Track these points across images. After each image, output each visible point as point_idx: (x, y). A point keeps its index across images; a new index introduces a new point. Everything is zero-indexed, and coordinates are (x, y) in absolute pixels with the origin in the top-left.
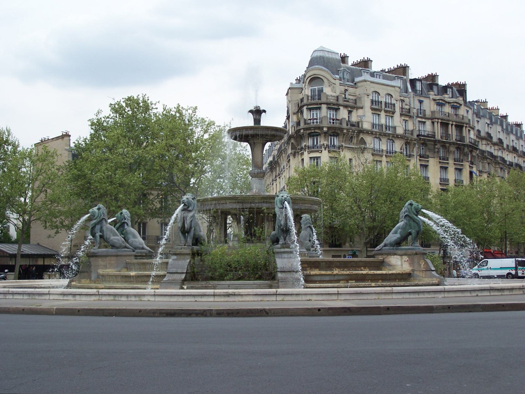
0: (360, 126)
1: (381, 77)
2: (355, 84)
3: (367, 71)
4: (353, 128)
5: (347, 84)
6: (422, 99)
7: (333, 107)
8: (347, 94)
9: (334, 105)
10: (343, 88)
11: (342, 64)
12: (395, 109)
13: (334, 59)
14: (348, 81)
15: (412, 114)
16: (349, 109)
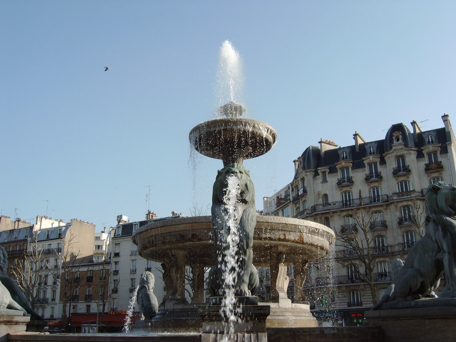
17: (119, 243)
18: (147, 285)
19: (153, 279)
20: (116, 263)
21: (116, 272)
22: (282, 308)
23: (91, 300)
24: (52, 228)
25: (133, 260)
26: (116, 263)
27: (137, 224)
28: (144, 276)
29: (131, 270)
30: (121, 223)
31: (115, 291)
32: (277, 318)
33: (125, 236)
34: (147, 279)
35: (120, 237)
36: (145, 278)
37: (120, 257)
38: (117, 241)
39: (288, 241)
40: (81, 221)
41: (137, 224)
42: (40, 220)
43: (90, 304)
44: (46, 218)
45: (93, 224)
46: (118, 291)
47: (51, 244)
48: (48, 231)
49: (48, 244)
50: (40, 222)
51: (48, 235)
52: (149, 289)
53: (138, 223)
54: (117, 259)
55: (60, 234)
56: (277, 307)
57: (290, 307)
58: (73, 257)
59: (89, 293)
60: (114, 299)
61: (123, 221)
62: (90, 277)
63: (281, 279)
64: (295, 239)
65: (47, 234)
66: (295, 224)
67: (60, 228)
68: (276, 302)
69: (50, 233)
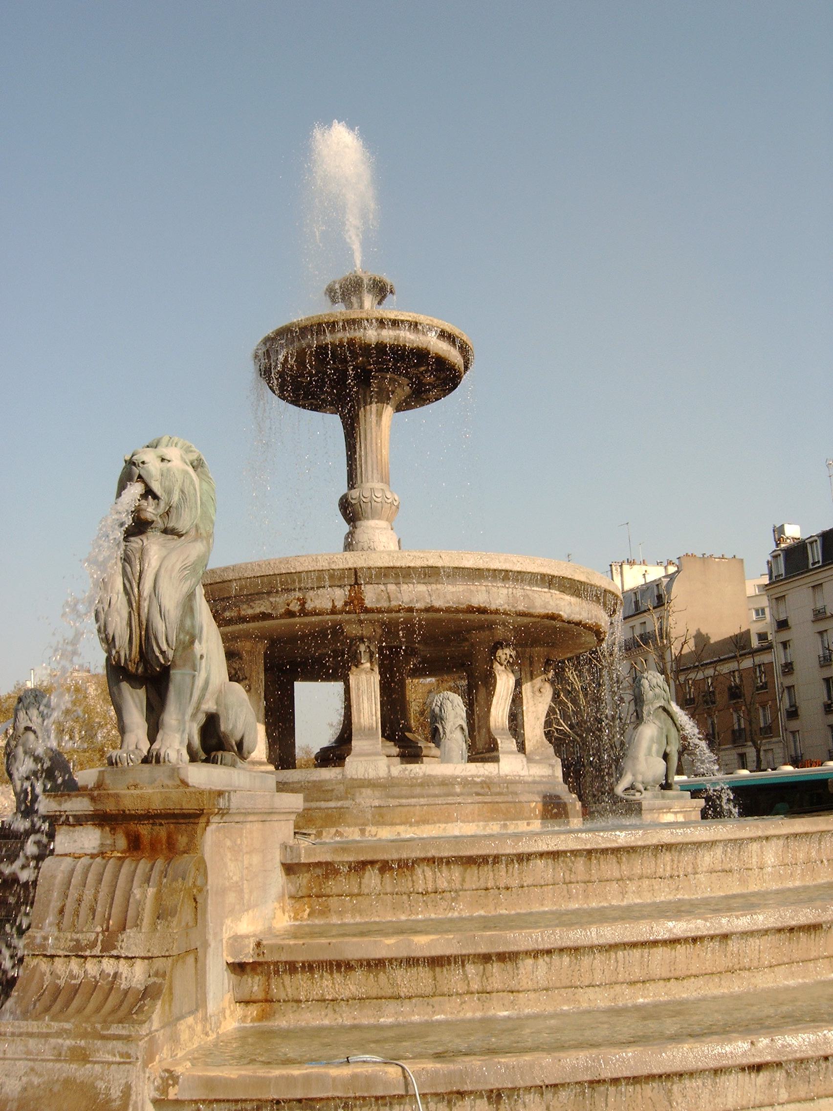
17: (784, 596)
18: (442, 723)
19: (458, 710)
20: (785, 645)
21: (788, 669)
22: (352, 779)
23: (746, 741)
24: (646, 584)
25: (821, 633)
26: (785, 645)
27: (816, 541)
28: (436, 705)
29: (819, 657)
30: (783, 545)
31: (793, 714)
32: (323, 804)
33: (799, 575)
34: (441, 711)
35: (782, 580)
36: (437, 709)
37: (790, 628)
38: (778, 591)
39: (314, 613)
40: (706, 556)
41: (816, 541)
42: (619, 570)
43: (744, 750)
44: (632, 563)
45: (737, 557)
46: (799, 713)
47: (645, 623)
48: (635, 593)
49: (641, 623)
50: (619, 575)
51: (636, 602)
52: (445, 733)
53: (816, 538)
54: (784, 636)
55: (660, 597)
56: (340, 777)
57: (382, 772)
58: (702, 639)
59: (765, 723)
60: (793, 733)
61: (788, 538)
62: (737, 687)
63: (366, 705)
64: (334, 607)
65: (633, 600)
66: (317, 568)
67: (657, 584)
68: (339, 766)
69: (639, 598)
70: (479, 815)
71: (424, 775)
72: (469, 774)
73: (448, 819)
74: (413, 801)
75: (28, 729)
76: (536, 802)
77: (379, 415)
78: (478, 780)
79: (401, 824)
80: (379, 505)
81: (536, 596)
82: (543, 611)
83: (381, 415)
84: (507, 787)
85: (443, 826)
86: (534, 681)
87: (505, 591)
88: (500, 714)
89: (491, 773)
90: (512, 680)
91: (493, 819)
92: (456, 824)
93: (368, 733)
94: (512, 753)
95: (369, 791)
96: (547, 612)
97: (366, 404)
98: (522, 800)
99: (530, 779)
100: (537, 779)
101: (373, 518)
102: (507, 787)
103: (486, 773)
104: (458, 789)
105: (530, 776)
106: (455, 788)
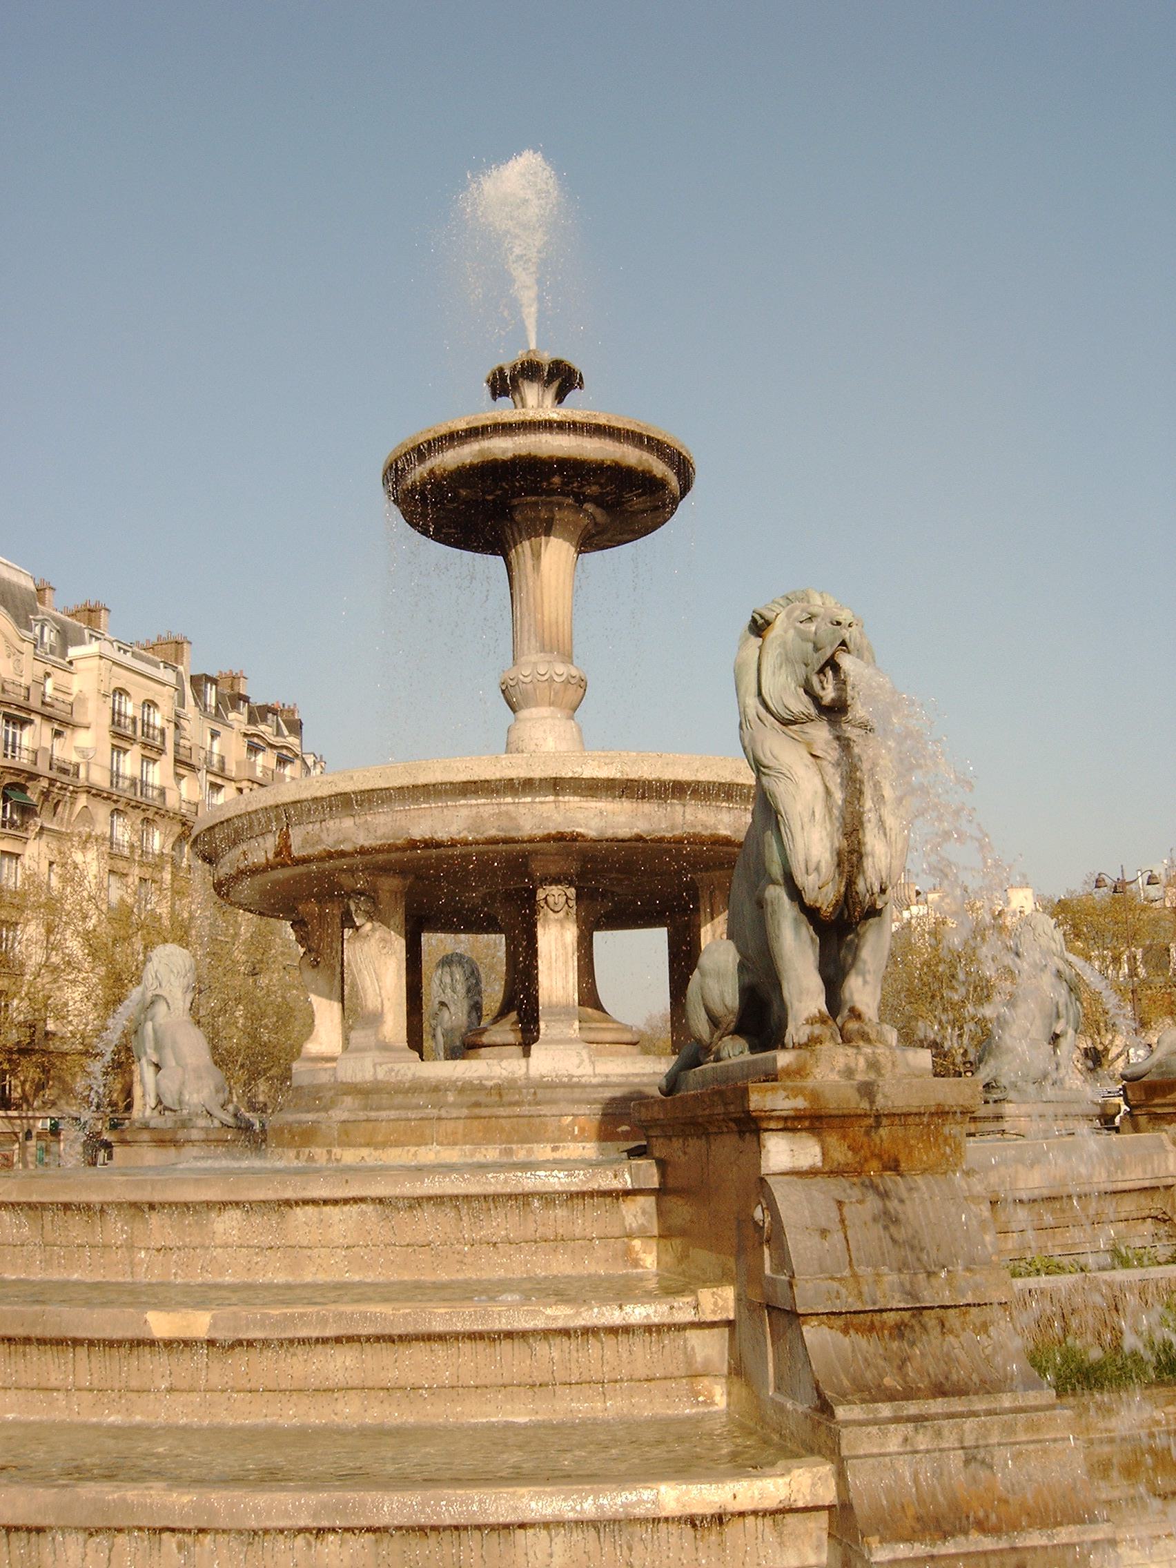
0: (82, 774)
1: (129, 654)
2: (71, 663)
3: (99, 636)
4: (65, 779)
5: (50, 660)
6: (217, 727)
7: (16, 713)
8: (49, 684)
9: (19, 707)
10: (40, 669)
11: (38, 604)
12: (163, 743)
13: (19, 587)
14: (52, 652)
15: (194, 761)
16: (56, 726)
56: (332, 1080)
70: (465, 1136)
71: (414, 1075)
72: (476, 1075)
73: (422, 1141)
74: (383, 1114)
75: (443, 1004)
76: (573, 1115)
77: (537, 556)
78: (490, 1083)
79: (368, 1145)
80: (530, 686)
81: (522, 810)
82: (540, 833)
83: (539, 555)
84: (535, 1093)
85: (413, 1149)
86: (716, 920)
87: (464, 812)
88: (560, 985)
89: (513, 1073)
90: (571, 933)
91: (489, 1141)
92: (431, 1147)
93: (562, 1012)
94: (570, 1041)
95: (348, 1100)
96: (546, 832)
97: (515, 545)
98: (548, 1114)
99: (595, 1081)
100: (614, 1079)
101: (527, 706)
102: (535, 1093)
103: (505, 1073)
104: (451, 1098)
105: (595, 1075)
106: (447, 1095)
